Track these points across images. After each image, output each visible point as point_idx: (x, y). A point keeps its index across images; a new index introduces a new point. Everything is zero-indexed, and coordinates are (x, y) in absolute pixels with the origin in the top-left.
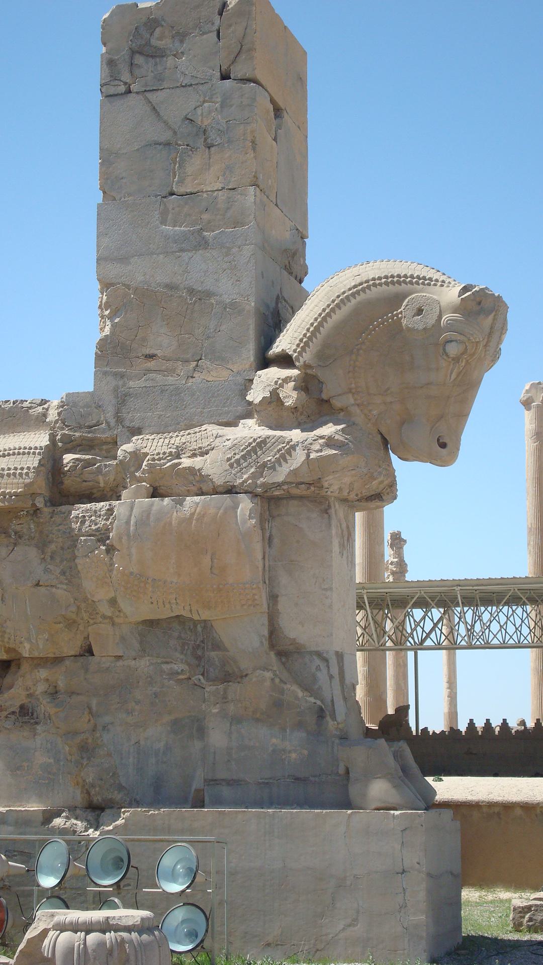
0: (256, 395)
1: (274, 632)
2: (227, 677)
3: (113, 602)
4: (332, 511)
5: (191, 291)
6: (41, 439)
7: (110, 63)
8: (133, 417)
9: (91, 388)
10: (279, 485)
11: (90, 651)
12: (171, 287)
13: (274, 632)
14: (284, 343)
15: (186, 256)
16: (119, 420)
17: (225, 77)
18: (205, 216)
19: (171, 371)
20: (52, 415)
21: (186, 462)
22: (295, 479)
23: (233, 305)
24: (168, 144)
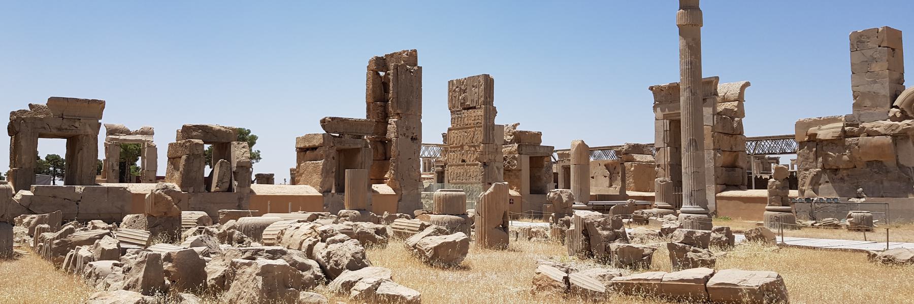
0: (891, 115)
1: (898, 163)
2: (888, 172)
3: (860, 158)
4: (910, 138)
5: (874, 93)
6: (841, 124)
7: (852, 44)
8: (862, 119)
9: (852, 113)
10: (896, 134)
11: (855, 167)
12: (869, 92)
13: (898, 163)
14: (896, 103)
15: (872, 85)
16: (859, 120)
17: (879, 46)
18: (877, 77)
19: (871, 109)
20: (843, 119)
21: (875, 129)
22: (900, 133)
23: (884, 95)
24: (866, 61)
